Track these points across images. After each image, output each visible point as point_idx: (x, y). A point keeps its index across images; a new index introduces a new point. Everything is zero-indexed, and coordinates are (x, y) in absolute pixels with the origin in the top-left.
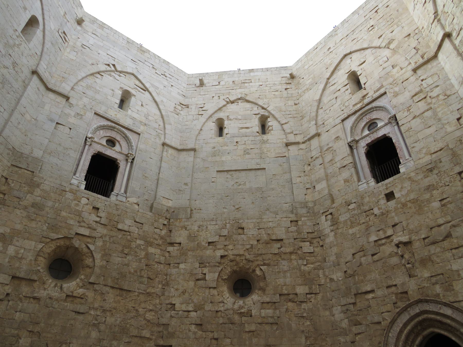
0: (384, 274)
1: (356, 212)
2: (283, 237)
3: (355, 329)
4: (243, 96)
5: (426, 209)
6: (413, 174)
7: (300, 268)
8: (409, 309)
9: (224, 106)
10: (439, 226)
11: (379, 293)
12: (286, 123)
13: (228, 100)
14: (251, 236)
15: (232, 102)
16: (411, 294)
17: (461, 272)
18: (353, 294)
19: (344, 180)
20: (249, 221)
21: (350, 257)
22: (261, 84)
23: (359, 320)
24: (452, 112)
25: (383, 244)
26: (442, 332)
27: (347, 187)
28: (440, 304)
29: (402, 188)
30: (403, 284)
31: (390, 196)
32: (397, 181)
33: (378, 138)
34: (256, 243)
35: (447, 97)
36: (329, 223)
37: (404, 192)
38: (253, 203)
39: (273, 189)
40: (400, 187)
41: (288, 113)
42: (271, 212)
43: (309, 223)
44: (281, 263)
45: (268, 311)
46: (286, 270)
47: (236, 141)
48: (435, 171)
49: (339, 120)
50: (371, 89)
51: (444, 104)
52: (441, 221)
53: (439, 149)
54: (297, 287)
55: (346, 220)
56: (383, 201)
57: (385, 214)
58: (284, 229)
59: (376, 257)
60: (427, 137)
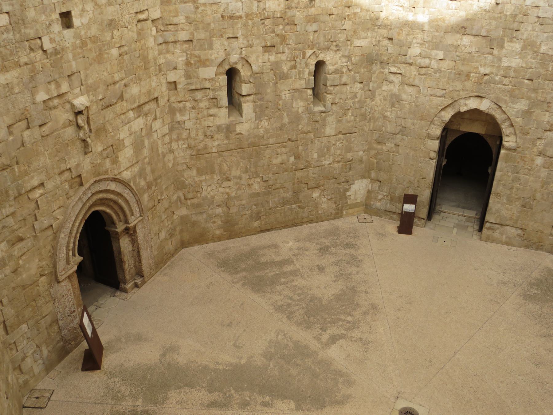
0: (56, 156)
1: (11, 36)
3: (16, 251)
10: (115, 83)
11: (49, 185)
17: (125, 141)
18: (12, 198)
25: (55, 107)
30: (78, 165)
37: (85, 20)
40: (81, 7)
52: (117, 77)
56: (57, 27)
59: (45, 129)
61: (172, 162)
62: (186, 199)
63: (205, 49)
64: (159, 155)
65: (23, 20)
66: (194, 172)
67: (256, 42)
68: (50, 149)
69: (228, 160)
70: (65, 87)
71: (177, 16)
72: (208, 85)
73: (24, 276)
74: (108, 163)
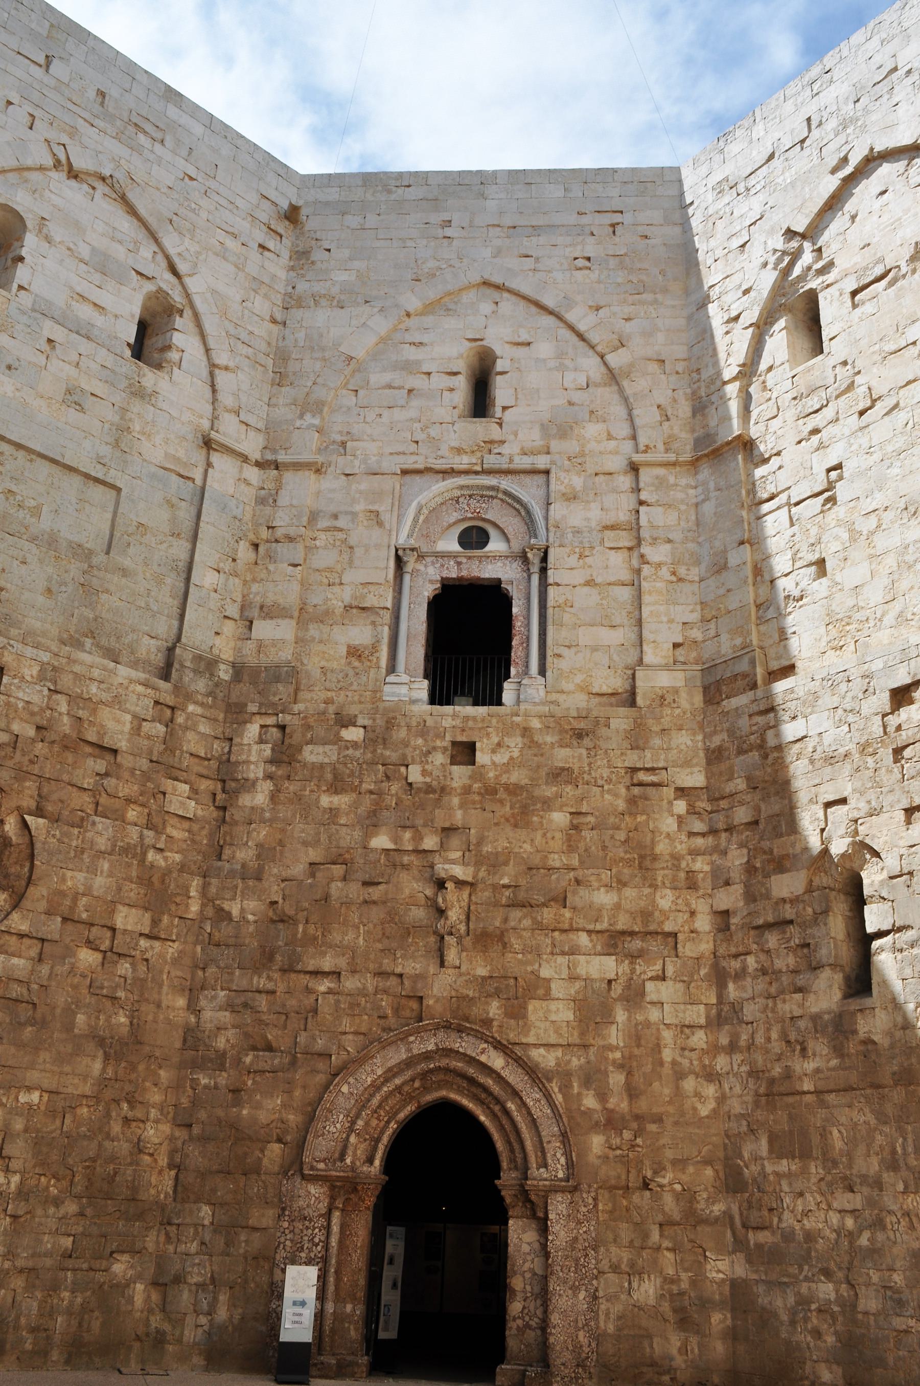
0: (379, 941)
1: (358, 754)
2: (123, 745)
4: (119, 175)
5: (535, 819)
6: (536, 724)
7: (144, 854)
8: (412, 1039)
9: (41, 168)
12: (227, 368)
13: (63, 158)
14: (21, 705)
15: (73, 174)
16: (428, 1006)
19: (349, 646)
20: (29, 652)
21: (298, 869)
22: (192, 172)
23: (270, 1037)
24: (671, 621)
26: (465, 1102)
27: (351, 673)
28: (486, 1042)
29: (499, 745)
31: (465, 752)
32: (494, 721)
33: (479, 578)
34: (31, 732)
35: (674, 579)
36: (267, 751)
37: (501, 758)
38: (49, 590)
39: (125, 572)
40: (496, 740)
41: (244, 336)
42: (98, 646)
43: (204, 728)
44: (94, 823)
45: (15, 960)
46: (103, 848)
47: (46, 333)
48: (586, 742)
49: (394, 464)
50: (516, 434)
51: (664, 592)
53: (610, 691)
54: (120, 907)
55: (322, 766)
56: (439, 759)
57: (434, 791)
58: (128, 717)
60: (595, 649)
61: (712, 1105)
62: (745, 1226)
63: (781, 836)
64: (661, 1063)
65: (384, 740)
66: (763, 1145)
67: (887, 800)
68: (371, 925)
69: (843, 1120)
70: (430, 842)
71: (731, 779)
72: (789, 912)
73: (245, 1112)
74: (494, 1009)
